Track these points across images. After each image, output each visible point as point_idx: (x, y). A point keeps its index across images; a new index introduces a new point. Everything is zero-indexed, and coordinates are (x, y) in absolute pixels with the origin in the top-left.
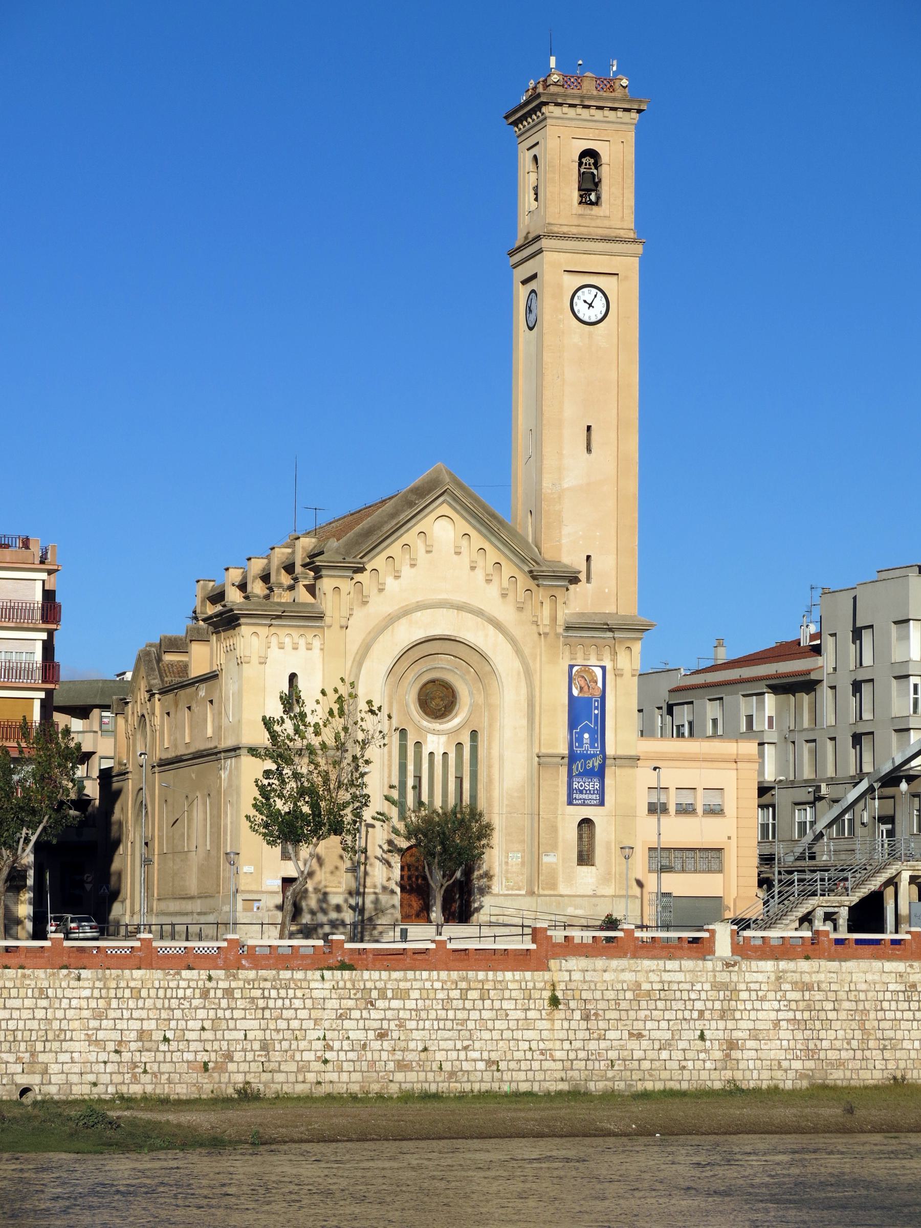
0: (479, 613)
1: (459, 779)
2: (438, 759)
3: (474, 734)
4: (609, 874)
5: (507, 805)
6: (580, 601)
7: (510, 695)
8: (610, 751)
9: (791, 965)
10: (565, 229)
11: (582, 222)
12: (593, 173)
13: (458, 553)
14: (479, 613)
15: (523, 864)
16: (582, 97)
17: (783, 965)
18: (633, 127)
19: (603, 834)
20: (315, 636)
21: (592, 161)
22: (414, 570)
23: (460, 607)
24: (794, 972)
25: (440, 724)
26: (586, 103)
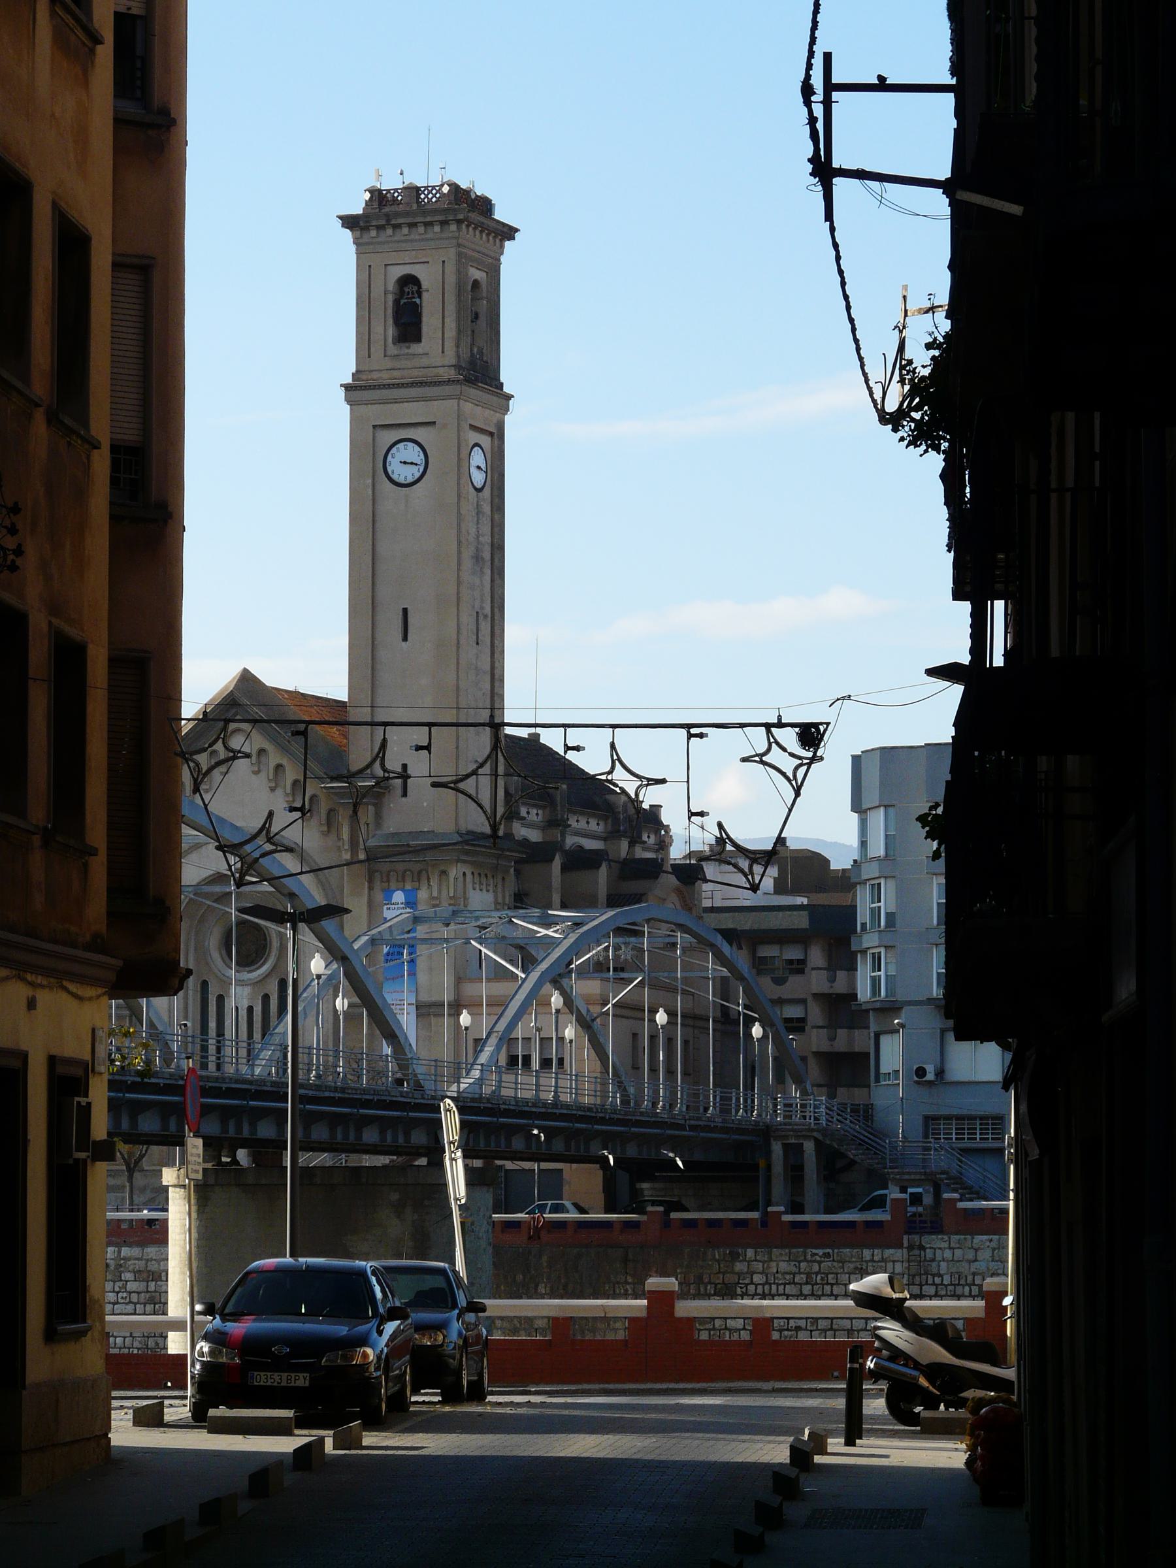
2: (243, 1014)
9: (135, 1252)
11: (398, 364)
17: (125, 1251)
21: (415, 288)
24: (138, 1259)
25: (249, 972)
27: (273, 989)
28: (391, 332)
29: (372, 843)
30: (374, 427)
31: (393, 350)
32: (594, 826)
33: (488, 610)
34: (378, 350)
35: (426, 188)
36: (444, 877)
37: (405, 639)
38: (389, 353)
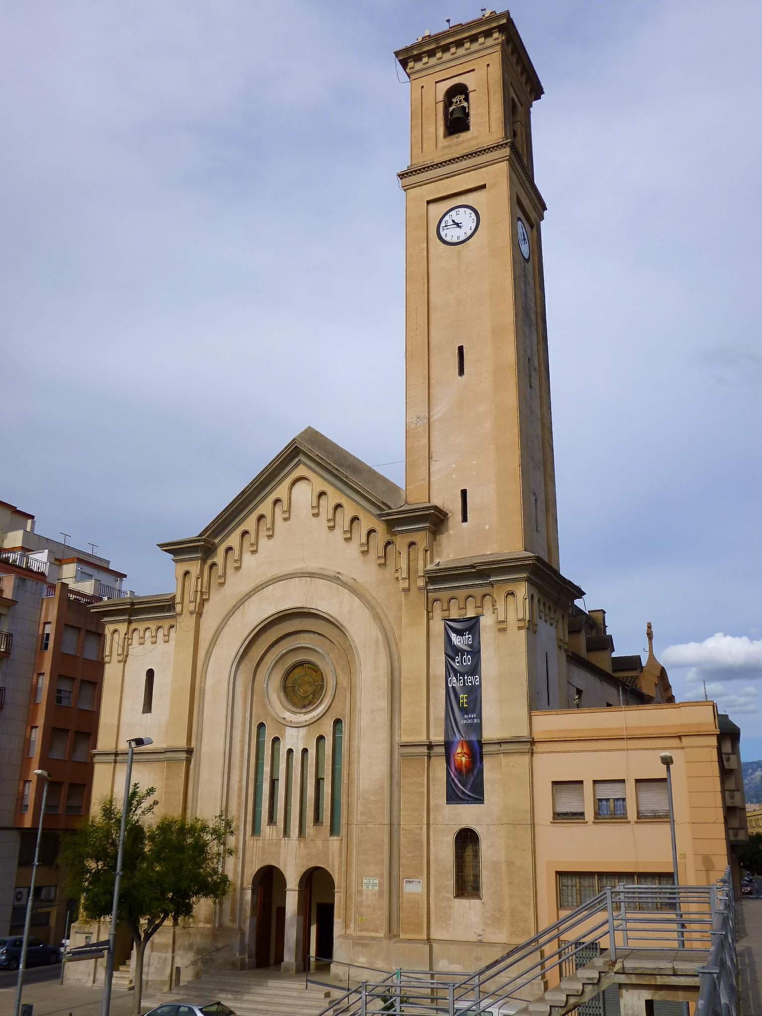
0: (336, 579)
1: (319, 781)
3: (338, 722)
4: (500, 910)
5: (361, 813)
6: (457, 547)
7: (371, 672)
8: (489, 733)
12: (464, 108)
13: (316, 515)
14: (336, 579)
15: (381, 893)
18: (498, 48)
19: (489, 851)
20: (172, 627)
22: (272, 541)
23: (312, 575)
25: (305, 713)
27: (327, 729)
28: (441, 130)
30: (428, 202)
31: (443, 142)
33: (536, 364)
34: (429, 145)
36: (510, 598)
37: (461, 372)
38: (440, 146)
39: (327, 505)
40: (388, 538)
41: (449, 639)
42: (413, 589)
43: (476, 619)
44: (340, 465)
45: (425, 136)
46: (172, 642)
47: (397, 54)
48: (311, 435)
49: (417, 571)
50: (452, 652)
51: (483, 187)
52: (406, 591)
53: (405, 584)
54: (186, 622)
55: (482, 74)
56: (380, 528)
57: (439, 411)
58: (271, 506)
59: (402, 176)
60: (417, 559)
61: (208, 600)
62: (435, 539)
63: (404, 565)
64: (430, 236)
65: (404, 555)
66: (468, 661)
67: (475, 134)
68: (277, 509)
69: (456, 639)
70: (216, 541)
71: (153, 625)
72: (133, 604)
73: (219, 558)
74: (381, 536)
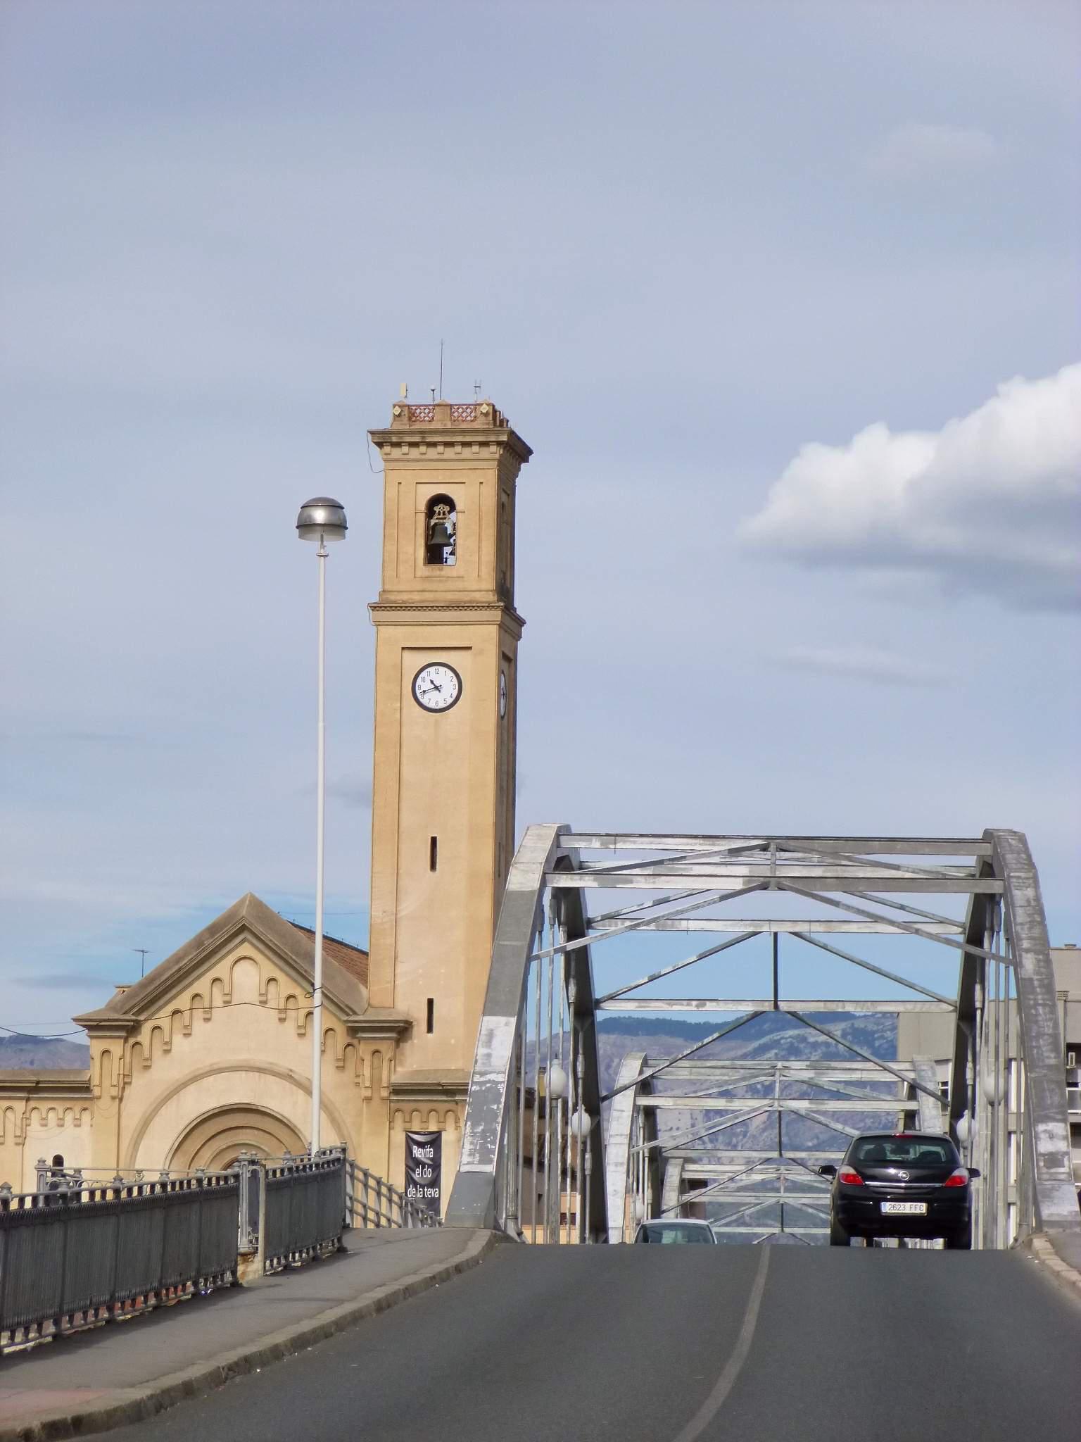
0: (289, 1077)
10: (405, 597)
11: (427, 586)
16: (422, 433)
20: (85, 1109)
22: (209, 1025)
23: (260, 1070)
26: (429, 440)
29: (396, 1079)
31: (423, 570)
32: (802, 1065)
35: (460, 406)
37: (433, 866)
38: (419, 574)
39: (277, 995)
40: (349, 1040)
41: (409, 1151)
42: (376, 1101)
43: (439, 1134)
44: (297, 954)
45: (401, 556)
46: (85, 1128)
47: (372, 433)
48: (257, 906)
49: (380, 1080)
50: (413, 1164)
51: (470, 648)
52: (368, 1099)
53: (368, 1093)
54: (105, 1105)
55: (473, 491)
56: (340, 1030)
57: (408, 906)
58: (209, 984)
59: (375, 608)
60: (380, 1067)
61: (130, 1083)
62: (397, 1046)
63: (367, 1072)
64: (404, 692)
65: (367, 1063)
66: (428, 1174)
67: (462, 573)
68: (214, 989)
69: (417, 1152)
70: (141, 1018)
71: (60, 1106)
72: (38, 1082)
73: (144, 1035)
74: (341, 1037)
